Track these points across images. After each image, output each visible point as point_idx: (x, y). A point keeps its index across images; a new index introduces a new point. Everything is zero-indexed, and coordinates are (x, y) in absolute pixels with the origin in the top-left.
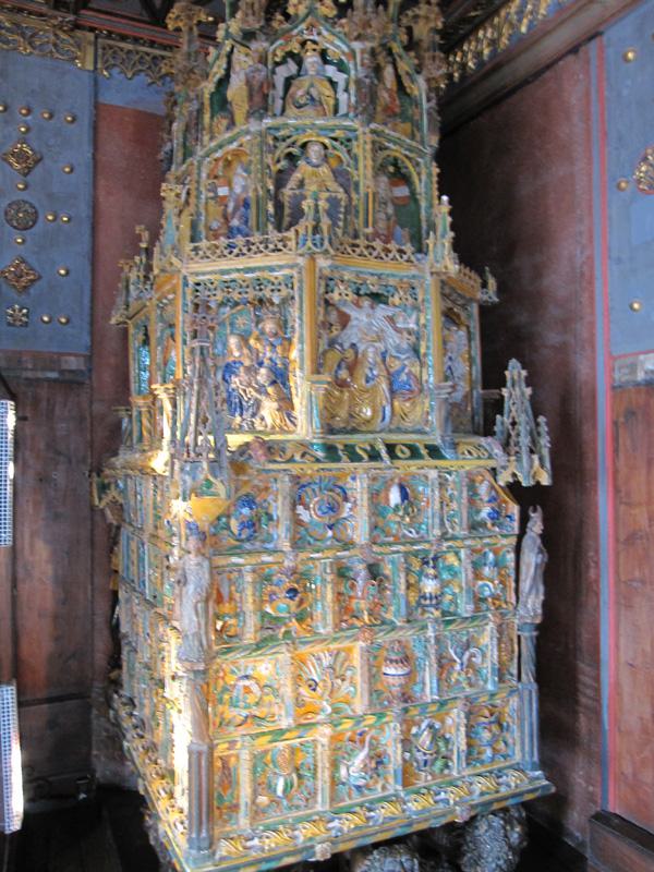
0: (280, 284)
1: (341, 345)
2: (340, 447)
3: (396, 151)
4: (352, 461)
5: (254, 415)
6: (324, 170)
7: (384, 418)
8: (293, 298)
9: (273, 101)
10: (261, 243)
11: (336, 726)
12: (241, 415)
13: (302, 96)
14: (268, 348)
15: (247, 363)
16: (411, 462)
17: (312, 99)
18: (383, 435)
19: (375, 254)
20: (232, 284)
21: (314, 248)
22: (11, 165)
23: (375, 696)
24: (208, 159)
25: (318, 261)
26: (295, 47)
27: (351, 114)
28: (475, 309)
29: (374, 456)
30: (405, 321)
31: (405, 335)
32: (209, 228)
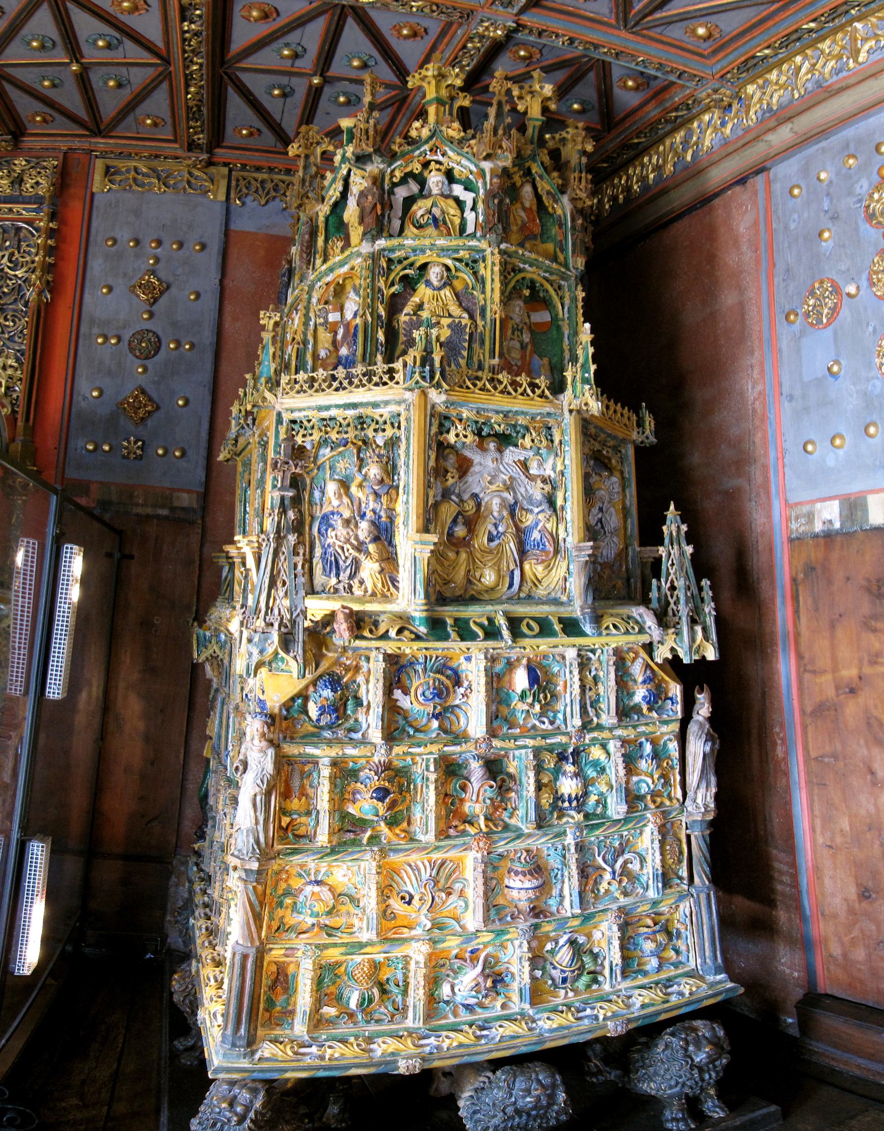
0: (385, 423)
1: (459, 496)
2: (449, 621)
3: (531, 273)
4: (463, 639)
5: (351, 577)
6: (447, 292)
7: (511, 585)
8: (398, 439)
9: (390, 221)
10: (364, 375)
11: (435, 942)
12: (338, 575)
13: (422, 216)
14: (371, 498)
15: (347, 514)
16: (539, 641)
17: (435, 220)
18: (507, 607)
19: (500, 388)
20: (331, 423)
21: (423, 383)
23: (493, 912)
24: (319, 284)
25: (430, 396)
26: (416, 167)
27: (478, 234)
29: (492, 633)
30: (540, 465)
31: (540, 484)
32: (315, 356)
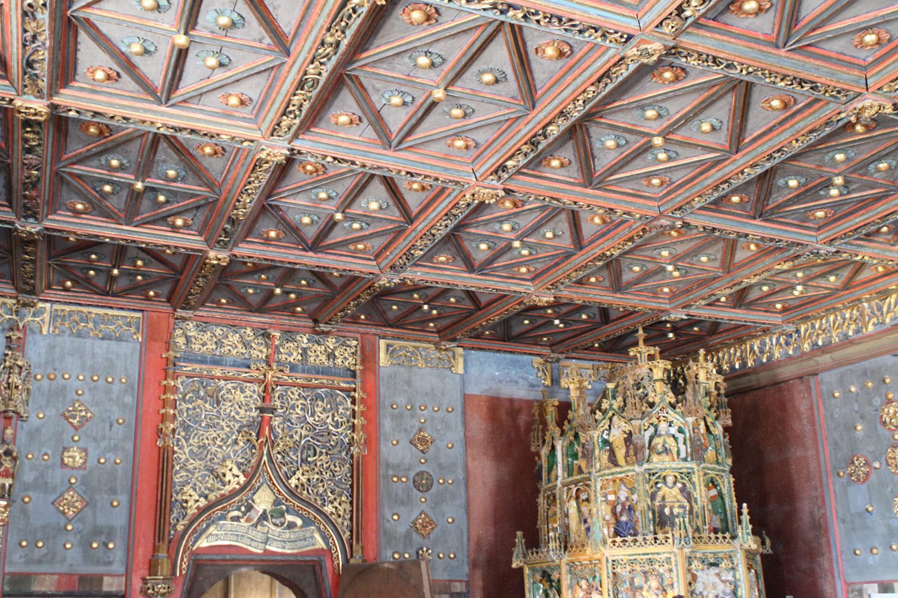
6: (676, 491)
27: (689, 459)
28: (758, 558)
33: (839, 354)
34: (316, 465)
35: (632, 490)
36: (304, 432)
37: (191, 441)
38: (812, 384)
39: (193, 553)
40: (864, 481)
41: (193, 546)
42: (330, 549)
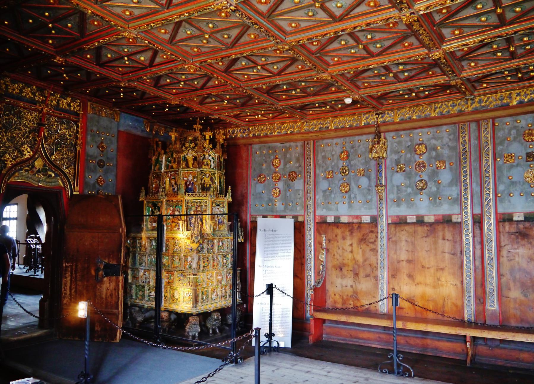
22: (100, 149)
33: (262, 140)
34: (61, 152)
35: (194, 177)
36: (57, 137)
37: (7, 134)
38: (249, 148)
39: (8, 184)
40: (263, 182)
41: (8, 180)
42: (65, 187)
